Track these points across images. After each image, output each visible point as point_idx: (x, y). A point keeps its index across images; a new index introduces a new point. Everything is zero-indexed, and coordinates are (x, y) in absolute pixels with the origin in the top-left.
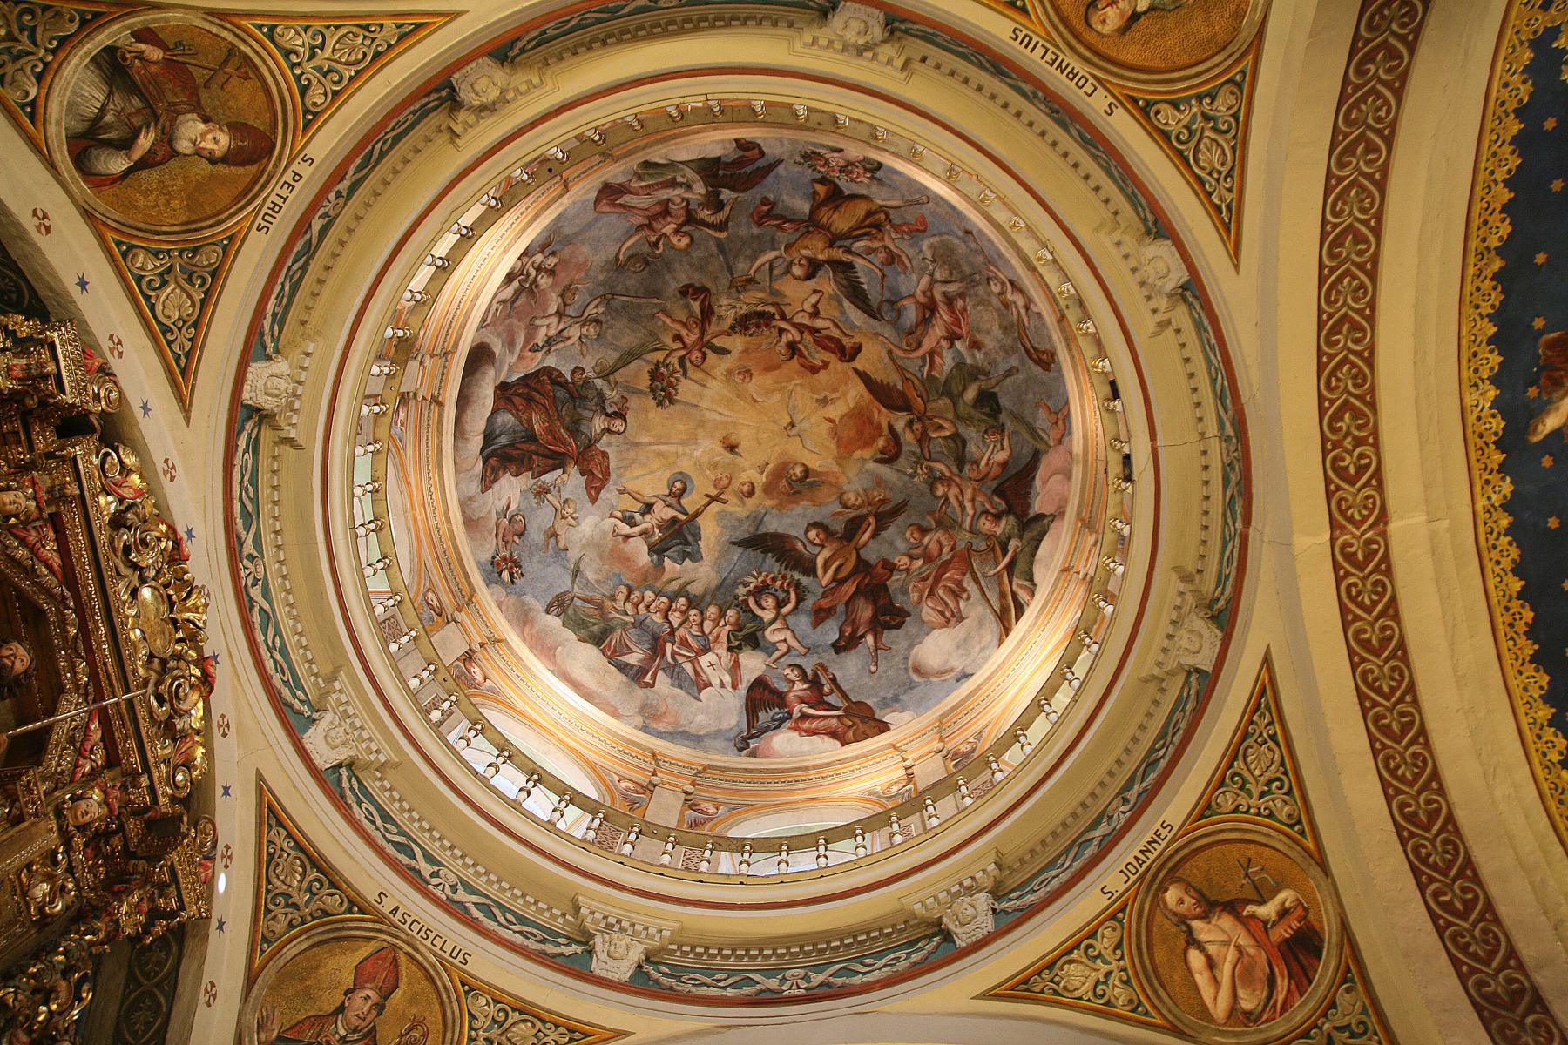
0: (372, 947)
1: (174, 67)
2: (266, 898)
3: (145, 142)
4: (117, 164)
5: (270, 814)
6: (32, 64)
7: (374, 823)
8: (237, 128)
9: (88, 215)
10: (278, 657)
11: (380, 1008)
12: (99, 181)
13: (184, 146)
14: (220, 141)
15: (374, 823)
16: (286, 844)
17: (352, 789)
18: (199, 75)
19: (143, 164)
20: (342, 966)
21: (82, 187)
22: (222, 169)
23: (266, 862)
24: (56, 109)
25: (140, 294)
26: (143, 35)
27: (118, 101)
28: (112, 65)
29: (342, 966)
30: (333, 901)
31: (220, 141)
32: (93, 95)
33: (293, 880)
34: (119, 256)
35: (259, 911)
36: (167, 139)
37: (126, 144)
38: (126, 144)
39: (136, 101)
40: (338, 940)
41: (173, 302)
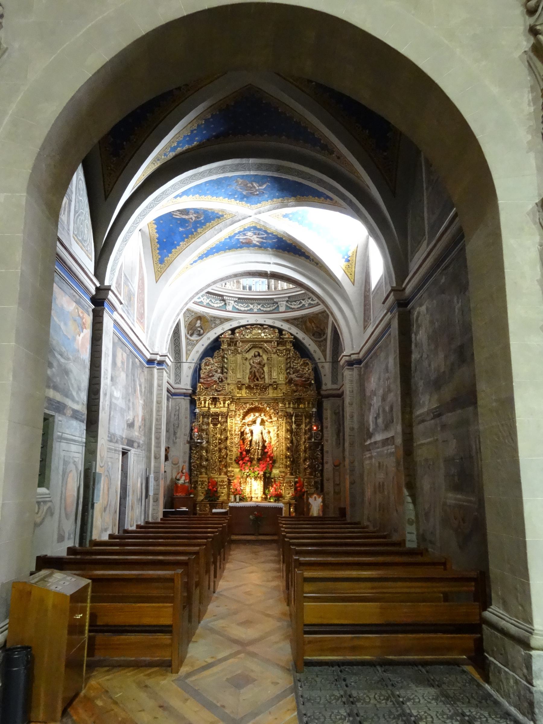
0: (308, 320)
1: (191, 329)
2: (297, 326)
3: (199, 329)
4: (202, 331)
5: (287, 321)
6: (192, 342)
7: (295, 305)
8: (197, 321)
9: (207, 333)
10: (268, 306)
11: (315, 324)
12: (204, 333)
13: (199, 325)
14: (199, 322)
15: (295, 305)
16: (292, 321)
17: (290, 304)
18: (192, 327)
19: (202, 329)
20: (308, 324)
21: (204, 334)
22: (202, 320)
23: (292, 324)
24: (197, 339)
25: (216, 326)
26: (188, 333)
27: (195, 333)
28: (191, 335)
29: (308, 324)
30: (300, 320)
31: (199, 322)
32: (195, 335)
33: (296, 322)
34: (212, 328)
35: (298, 327)
36: (199, 327)
37: (200, 331)
38: (200, 331)
39: (195, 331)
40: (305, 323)
41: (218, 322)
